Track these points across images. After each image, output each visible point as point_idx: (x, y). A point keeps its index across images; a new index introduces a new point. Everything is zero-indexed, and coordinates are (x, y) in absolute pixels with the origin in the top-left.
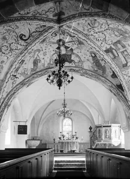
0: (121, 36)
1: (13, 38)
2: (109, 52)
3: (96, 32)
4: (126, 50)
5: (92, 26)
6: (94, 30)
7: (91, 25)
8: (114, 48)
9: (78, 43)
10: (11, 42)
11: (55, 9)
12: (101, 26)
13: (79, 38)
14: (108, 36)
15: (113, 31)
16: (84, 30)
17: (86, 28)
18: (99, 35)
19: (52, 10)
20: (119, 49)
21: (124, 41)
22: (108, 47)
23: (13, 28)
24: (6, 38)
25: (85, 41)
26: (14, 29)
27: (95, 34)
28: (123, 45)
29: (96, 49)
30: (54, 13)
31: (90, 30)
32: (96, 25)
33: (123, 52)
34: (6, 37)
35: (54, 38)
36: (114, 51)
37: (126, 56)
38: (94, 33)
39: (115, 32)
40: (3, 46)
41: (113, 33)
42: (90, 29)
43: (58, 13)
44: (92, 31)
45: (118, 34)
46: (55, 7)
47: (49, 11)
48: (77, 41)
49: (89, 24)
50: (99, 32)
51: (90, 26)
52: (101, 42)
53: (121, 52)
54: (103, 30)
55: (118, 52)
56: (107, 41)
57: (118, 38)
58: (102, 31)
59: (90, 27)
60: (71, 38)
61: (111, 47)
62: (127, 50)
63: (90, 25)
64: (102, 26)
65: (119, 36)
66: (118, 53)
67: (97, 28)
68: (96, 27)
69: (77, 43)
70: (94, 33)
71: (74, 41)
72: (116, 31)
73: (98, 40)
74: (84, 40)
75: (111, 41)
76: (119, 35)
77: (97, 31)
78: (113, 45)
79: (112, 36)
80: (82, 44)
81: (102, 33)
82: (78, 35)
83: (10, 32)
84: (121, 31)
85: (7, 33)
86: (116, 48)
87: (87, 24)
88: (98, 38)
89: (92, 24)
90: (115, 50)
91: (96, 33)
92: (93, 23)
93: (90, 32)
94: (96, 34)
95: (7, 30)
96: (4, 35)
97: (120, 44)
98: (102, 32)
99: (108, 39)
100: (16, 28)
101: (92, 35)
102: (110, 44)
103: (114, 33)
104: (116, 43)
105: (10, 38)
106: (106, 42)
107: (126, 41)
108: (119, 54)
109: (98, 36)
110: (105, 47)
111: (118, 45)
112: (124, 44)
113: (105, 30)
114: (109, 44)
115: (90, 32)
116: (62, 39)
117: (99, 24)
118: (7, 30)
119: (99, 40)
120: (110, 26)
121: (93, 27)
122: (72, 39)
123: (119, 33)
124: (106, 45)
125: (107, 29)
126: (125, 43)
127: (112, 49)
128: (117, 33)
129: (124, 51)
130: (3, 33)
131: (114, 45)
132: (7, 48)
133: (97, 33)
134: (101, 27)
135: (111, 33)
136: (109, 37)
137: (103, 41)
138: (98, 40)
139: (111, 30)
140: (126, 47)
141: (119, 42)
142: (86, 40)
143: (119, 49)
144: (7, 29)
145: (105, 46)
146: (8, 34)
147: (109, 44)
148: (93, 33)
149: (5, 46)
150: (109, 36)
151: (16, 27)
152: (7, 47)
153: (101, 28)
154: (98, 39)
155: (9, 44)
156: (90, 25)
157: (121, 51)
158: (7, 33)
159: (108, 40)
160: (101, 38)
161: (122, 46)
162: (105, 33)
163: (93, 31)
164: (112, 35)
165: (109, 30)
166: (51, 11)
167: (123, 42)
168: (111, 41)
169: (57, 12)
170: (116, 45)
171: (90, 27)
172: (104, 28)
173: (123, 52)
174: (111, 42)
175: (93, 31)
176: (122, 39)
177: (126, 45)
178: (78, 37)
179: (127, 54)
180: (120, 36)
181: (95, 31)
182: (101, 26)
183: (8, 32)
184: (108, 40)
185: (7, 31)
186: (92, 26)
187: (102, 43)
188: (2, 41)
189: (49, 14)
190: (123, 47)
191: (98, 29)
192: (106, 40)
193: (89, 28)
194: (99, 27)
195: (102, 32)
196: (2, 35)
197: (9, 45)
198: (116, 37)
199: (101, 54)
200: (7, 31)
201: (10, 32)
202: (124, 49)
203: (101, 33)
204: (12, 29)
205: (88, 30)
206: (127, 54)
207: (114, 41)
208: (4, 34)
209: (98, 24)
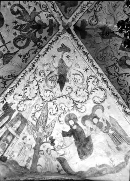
0: (35, 123)
2: (4, 110)
3: (39, 83)
4: (14, 137)
5: (48, 77)
6: (43, 80)
7: (50, 76)
8: (12, 118)
9: (4, 53)
11: (92, 25)
12: (49, 90)
13: (38, 58)
14: (32, 102)
15: (40, 109)
16: (44, 65)
17: (45, 68)
18: (34, 88)
19: (93, 22)
20: (12, 126)
21: (27, 129)
22: (13, 107)
25: (30, 68)
27: (35, 83)
28: (20, 129)
29: (16, 87)
30: (88, 23)
31: (42, 74)
32: (49, 83)
33: (9, 134)
35: (9, 7)
36: (8, 117)
37: (4, 141)
38: (37, 81)
39: (40, 112)
41: (38, 109)
42: (45, 75)
43: (85, 29)
44: (41, 78)
45: (38, 118)
46: (94, 27)
47: (94, 17)
48: (9, 51)
49: (52, 72)
50: (38, 88)
51: (48, 75)
52: (22, 93)
53: (8, 130)
54: (41, 95)
55: (7, 125)
56: (24, 103)
57: (30, 119)
58: (40, 93)
59: (46, 76)
60: (12, 41)
61: (13, 111)
62: (15, 138)
63: (50, 73)
64: (50, 91)
65: (33, 120)
66: (5, 126)
67: (45, 85)
68: (46, 83)
69: (4, 50)
70: (37, 81)
71: (5, 45)
72: (42, 113)
73: (26, 87)
74: (34, 66)
75: (23, 109)
76: (35, 119)
77: (41, 85)
78: (18, 114)
79: (32, 108)
80: (3, 60)
81: (36, 94)
82: (44, 55)
84: (44, 121)
86: (12, 121)
87: (53, 69)
88: (28, 88)
89: (52, 77)
90: (9, 120)
91: (37, 84)
92: (53, 77)
93: (40, 75)
94: (36, 84)
97: (21, 124)
98: (38, 94)
99: (27, 104)
101: (34, 78)
102: (19, 109)
103: (38, 111)
104: (22, 117)
106: (22, 102)
107: (29, 132)
108: (3, 128)
109: (32, 87)
110: (13, 101)
111: (19, 122)
112: (22, 130)
113: (41, 96)
114: (18, 107)
115: (40, 75)
116: (5, 23)
117: (52, 88)
119: (26, 91)
120: (50, 104)
121: (47, 78)
122: (10, 42)
123: (39, 118)
124: (17, 102)
125: (43, 99)
126: (25, 130)
127: (10, 114)
128: (38, 115)
129: (12, 134)
131: (17, 116)
133: (36, 85)
134: (46, 91)
135: (37, 106)
136: (30, 104)
137: (23, 97)
138: (26, 87)
139: (43, 105)
140: (19, 135)
141: (25, 121)
142: (33, 68)
143: (12, 126)
145: (15, 101)
147: (18, 107)
148: (38, 79)
150: (31, 105)
153: (45, 90)
154: (26, 89)
156: (50, 73)
157: (10, 129)
159: (25, 105)
160: (28, 92)
161: (19, 128)
162: (36, 98)
163: (40, 79)
164: (34, 109)
165: (43, 103)
166: (93, 19)
167: (26, 127)
168: (23, 109)
169: (87, 27)
170: (18, 119)
171: (46, 76)
172: (46, 94)
173: (9, 133)
174: (22, 110)
175: (40, 79)
176: (31, 124)
177: (22, 133)
178: (39, 55)
179: (10, 141)
180: (35, 120)
181: (41, 82)
182: (49, 90)
184: (25, 105)
186: (48, 77)
187: (20, 95)
189: (90, 16)
190: (17, 130)
191: (44, 86)
192: (24, 100)
193: (46, 72)
194: (47, 88)
195: (38, 94)
198: (31, 115)
199: (6, 96)
202: (14, 134)
203: (36, 92)
205: (43, 71)
206: (10, 141)
207: (24, 115)
209: (52, 86)
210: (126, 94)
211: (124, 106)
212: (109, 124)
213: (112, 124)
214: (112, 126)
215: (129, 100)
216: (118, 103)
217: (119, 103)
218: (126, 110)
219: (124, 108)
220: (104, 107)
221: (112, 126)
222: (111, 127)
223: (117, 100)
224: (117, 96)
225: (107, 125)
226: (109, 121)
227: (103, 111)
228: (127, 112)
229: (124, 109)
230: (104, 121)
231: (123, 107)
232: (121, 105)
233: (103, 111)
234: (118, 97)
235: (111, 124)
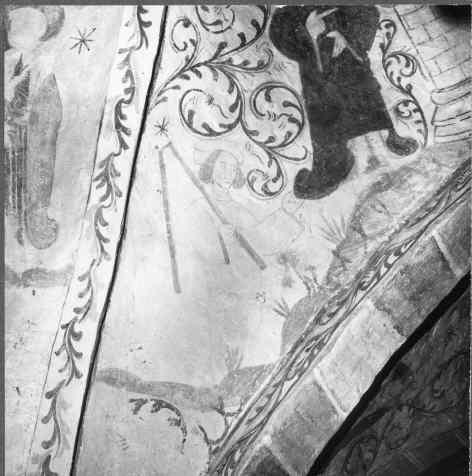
210: (188, 61)
211: (131, 90)
212: (23, 104)
213: (34, 117)
214: (26, 117)
215: (177, 87)
216: (125, 55)
217: (127, 59)
218: (125, 110)
219: (127, 97)
220: (63, 31)
221: (26, 117)
222: (17, 120)
223: (130, 45)
224: (145, 29)
225: (16, 98)
226: (35, 88)
227: (45, 38)
228: (122, 122)
229: (122, 101)
230: (17, 72)
231: (127, 91)
232: (129, 74)
233: (45, 38)
234: (143, 34)
235: (29, 108)
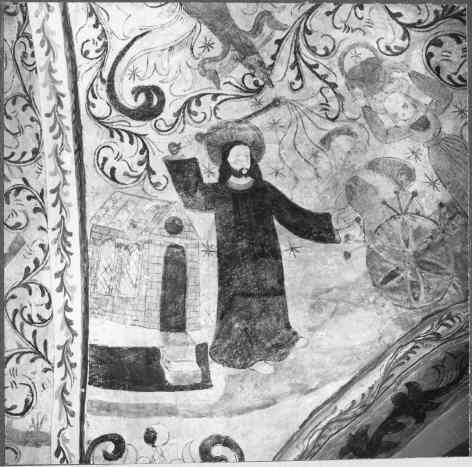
1: (354, 23)
10: (394, 22)
23: (279, 42)
24: (366, 62)
26: (279, 35)
34: (352, 71)
40: (438, 70)
83: (313, 50)
85: (321, 71)
95: (300, 76)
96: (341, 82)
100: (277, 26)
105: (358, 37)
118: (300, 76)
130: (330, 93)
132: (449, 42)
144: (293, 74)
146: (335, 59)
149: (429, 56)
151: (266, 30)
152: (437, 43)
155: (406, 36)
158: (321, 71)
183: (311, 67)
185: (305, 70)
188: (389, 88)
196: (340, 97)
197: (412, 32)
200: (305, 70)
201: (313, 50)
204: (287, 45)
208: (333, 86)
